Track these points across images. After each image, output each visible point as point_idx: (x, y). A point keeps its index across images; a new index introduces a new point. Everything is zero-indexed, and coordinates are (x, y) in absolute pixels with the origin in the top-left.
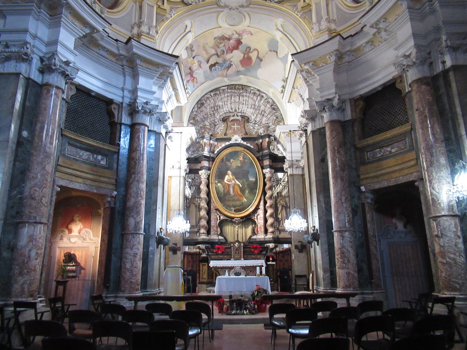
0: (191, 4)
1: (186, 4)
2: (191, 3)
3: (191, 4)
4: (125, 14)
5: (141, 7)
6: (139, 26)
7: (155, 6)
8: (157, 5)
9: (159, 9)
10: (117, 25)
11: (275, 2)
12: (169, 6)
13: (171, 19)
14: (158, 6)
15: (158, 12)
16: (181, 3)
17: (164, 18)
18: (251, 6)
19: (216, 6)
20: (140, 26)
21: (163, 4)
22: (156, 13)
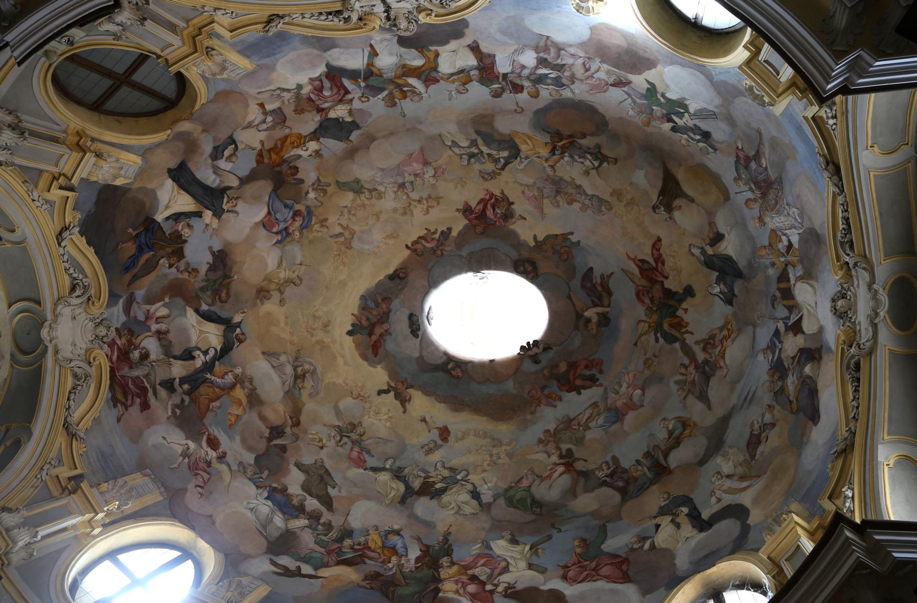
0: (59, 245)
1: (60, 234)
2: (63, 244)
3: (59, 245)
4: (42, 104)
5: (55, 140)
6: (13, 127)
7: (55, 170)
8: (60, 175)
9: (51, 177)
10: (18, 80)
11: (66, 419)
12: (55, 199)
13: (30, 201)
14: (57, 175)
15: (45, 175)
16: (63, 225)
17: (31, 187)
18: (57, 368)
19: (56, 296)
20: (13, 129)
21: (61, 188)
22: (41, 171)
